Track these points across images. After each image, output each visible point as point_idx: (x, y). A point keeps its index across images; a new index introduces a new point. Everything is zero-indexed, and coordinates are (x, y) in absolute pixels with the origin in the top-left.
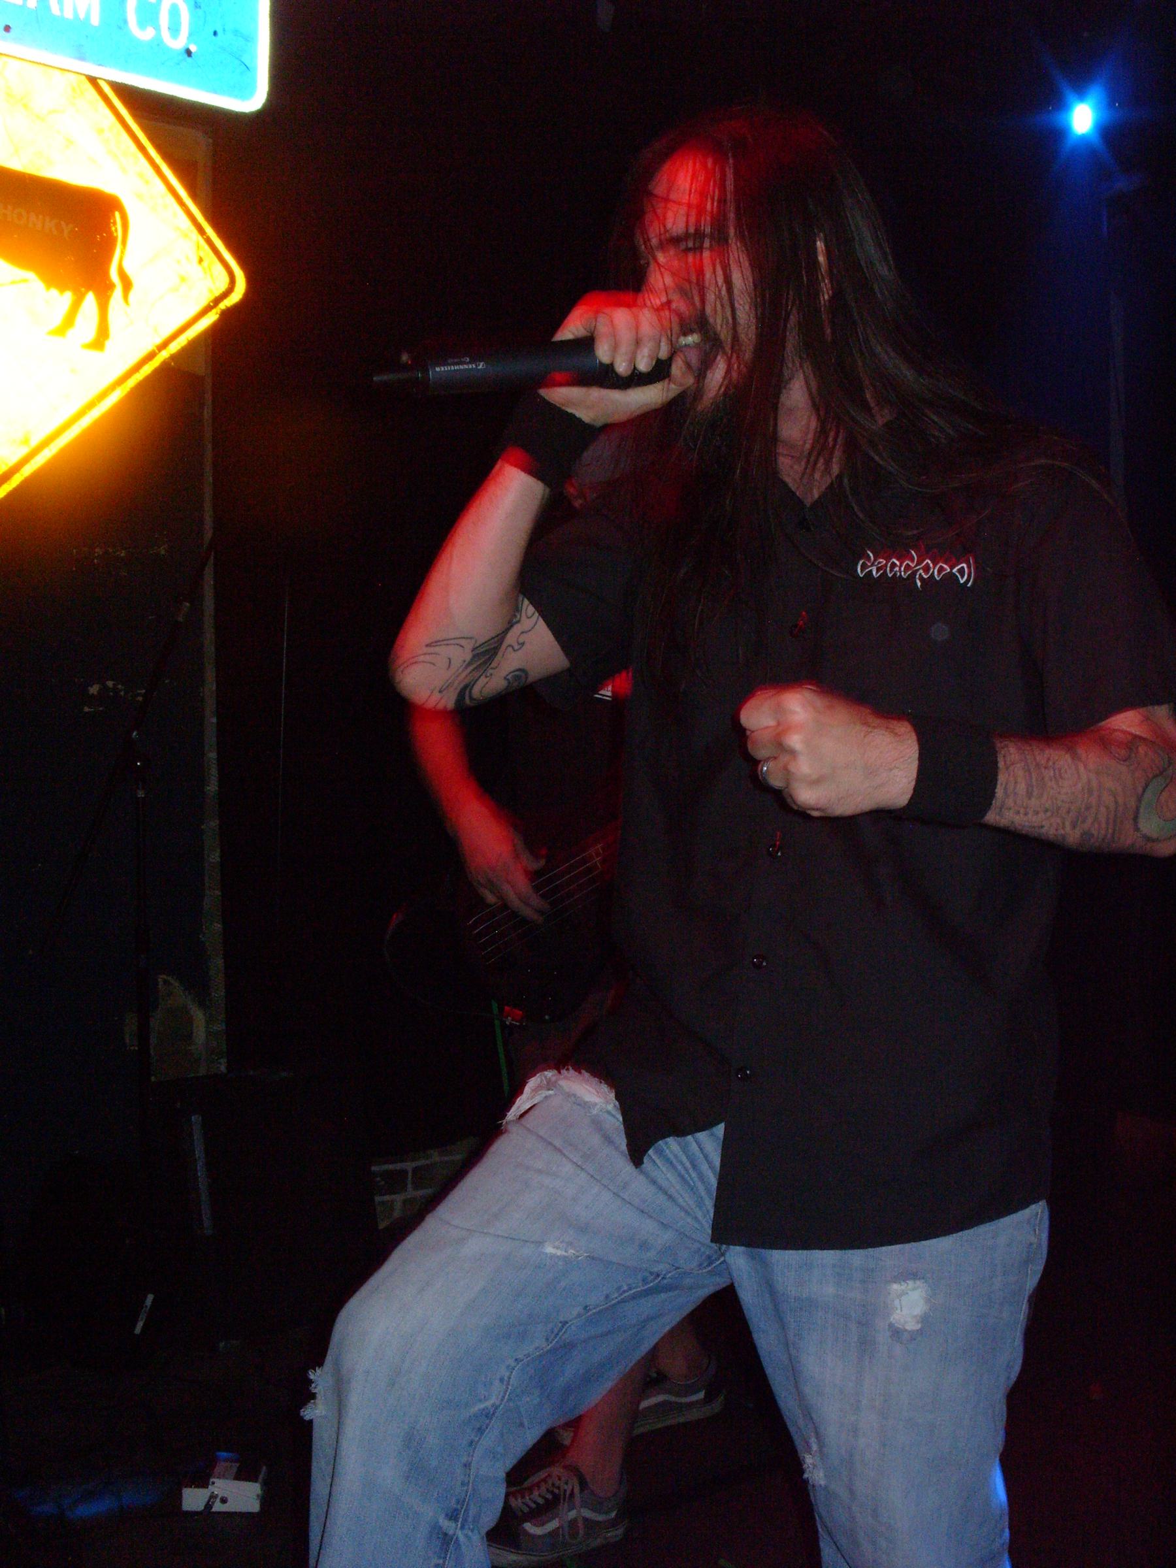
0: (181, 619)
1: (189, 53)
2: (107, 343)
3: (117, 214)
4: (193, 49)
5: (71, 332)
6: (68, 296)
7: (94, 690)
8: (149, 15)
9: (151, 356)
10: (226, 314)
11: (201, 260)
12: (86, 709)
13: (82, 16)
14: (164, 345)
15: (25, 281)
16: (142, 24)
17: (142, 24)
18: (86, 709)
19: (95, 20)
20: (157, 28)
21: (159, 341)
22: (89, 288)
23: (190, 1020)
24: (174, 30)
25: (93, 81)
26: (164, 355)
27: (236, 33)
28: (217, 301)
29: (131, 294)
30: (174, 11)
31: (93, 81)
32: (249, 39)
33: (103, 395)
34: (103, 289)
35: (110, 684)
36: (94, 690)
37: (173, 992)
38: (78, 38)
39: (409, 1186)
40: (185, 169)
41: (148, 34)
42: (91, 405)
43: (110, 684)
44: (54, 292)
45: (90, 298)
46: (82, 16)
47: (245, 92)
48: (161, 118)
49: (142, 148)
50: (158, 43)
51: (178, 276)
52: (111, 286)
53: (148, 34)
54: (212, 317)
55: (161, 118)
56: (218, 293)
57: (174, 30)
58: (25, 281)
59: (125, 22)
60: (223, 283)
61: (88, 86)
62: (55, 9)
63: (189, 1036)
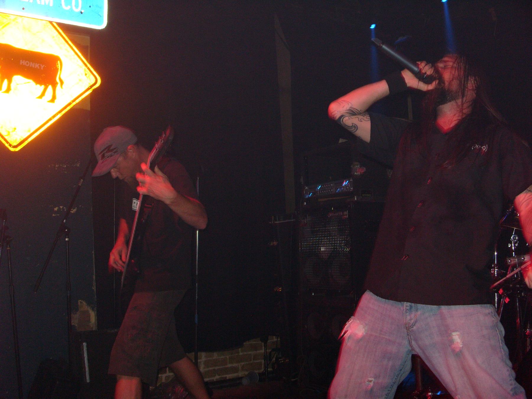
0: (80, 185)
1: (81, 13)
2: (55, 100)
3: (59, 62)
4: (83, 11)
5: (43, 97)
6: (43, 87)
7: (56, 209)
8: (68, 1)
9: (70, 104)
10: (94, 91)
11: (86, 74)
12: (53, 215)
13: (47, 4)
14: (74, 101)
15: (28, 83)
16: (66, 5)
17: (66, 5)
18: (53, 215)
19: (51, 4)
21: (73, 99)
22: (49, 84)
23: (89, 316)
24: (77, 6)
25: (51, 22)
26: (74, 103)
28: (91, 86)
29: (63, 86)
31: (51, 22)
32: (101, 8)
33: (54, 117)
34: (54, 85)
35: (61, 207)
36: (56, 209)
37: (84, 306)
39: (168, 371)
40: (83, 49)
41: (68, 8)
42: (50, 119)
43: (61, 207)
44: (38, 85)
45: (50, 87)
46: (47, 4)
47: (101, 23)
48: (72, 32)
49: (67, 42)
50: (71, 10)
51: (79, 79)
52: (57, 83)
53: (68, 8)
54: (90, 91)
55: (72, 32)
56: (91, 84)
57: (77, 6)
58: (28, 83)
59: (61, 5)
60: (93, 81)
61: (50, 24)
62: (39, 2)
63: (89, 321)
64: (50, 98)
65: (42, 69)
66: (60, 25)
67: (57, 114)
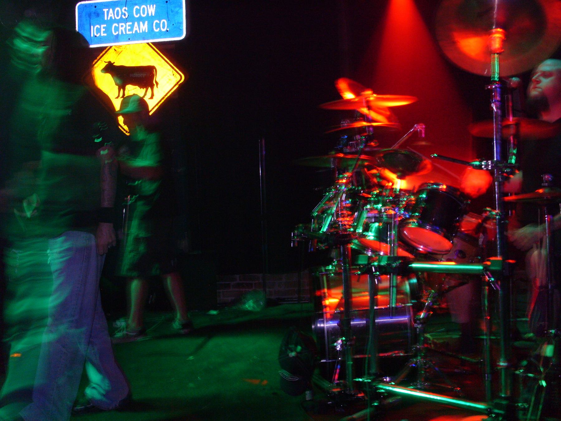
6: (145, 89)
9: (163, 98)
16: (156, 29)
19: (147, 31)
20: (160, 28)
24: (164, 27)
25: (148, 44)
26: (167, 97)
27: (178, 23)
29: (158, 86)
30: (164, 23)
31: (148, 44)
38: (143, 36)
44: (142, 89)
45: (149, 89)
47: (180, 35)
50: (160, 30)
52: (154, 85)
57: (164, 27)
64: (150, 96)
65: (144, 76)
66: (153, 43)
67: (155, 106)
